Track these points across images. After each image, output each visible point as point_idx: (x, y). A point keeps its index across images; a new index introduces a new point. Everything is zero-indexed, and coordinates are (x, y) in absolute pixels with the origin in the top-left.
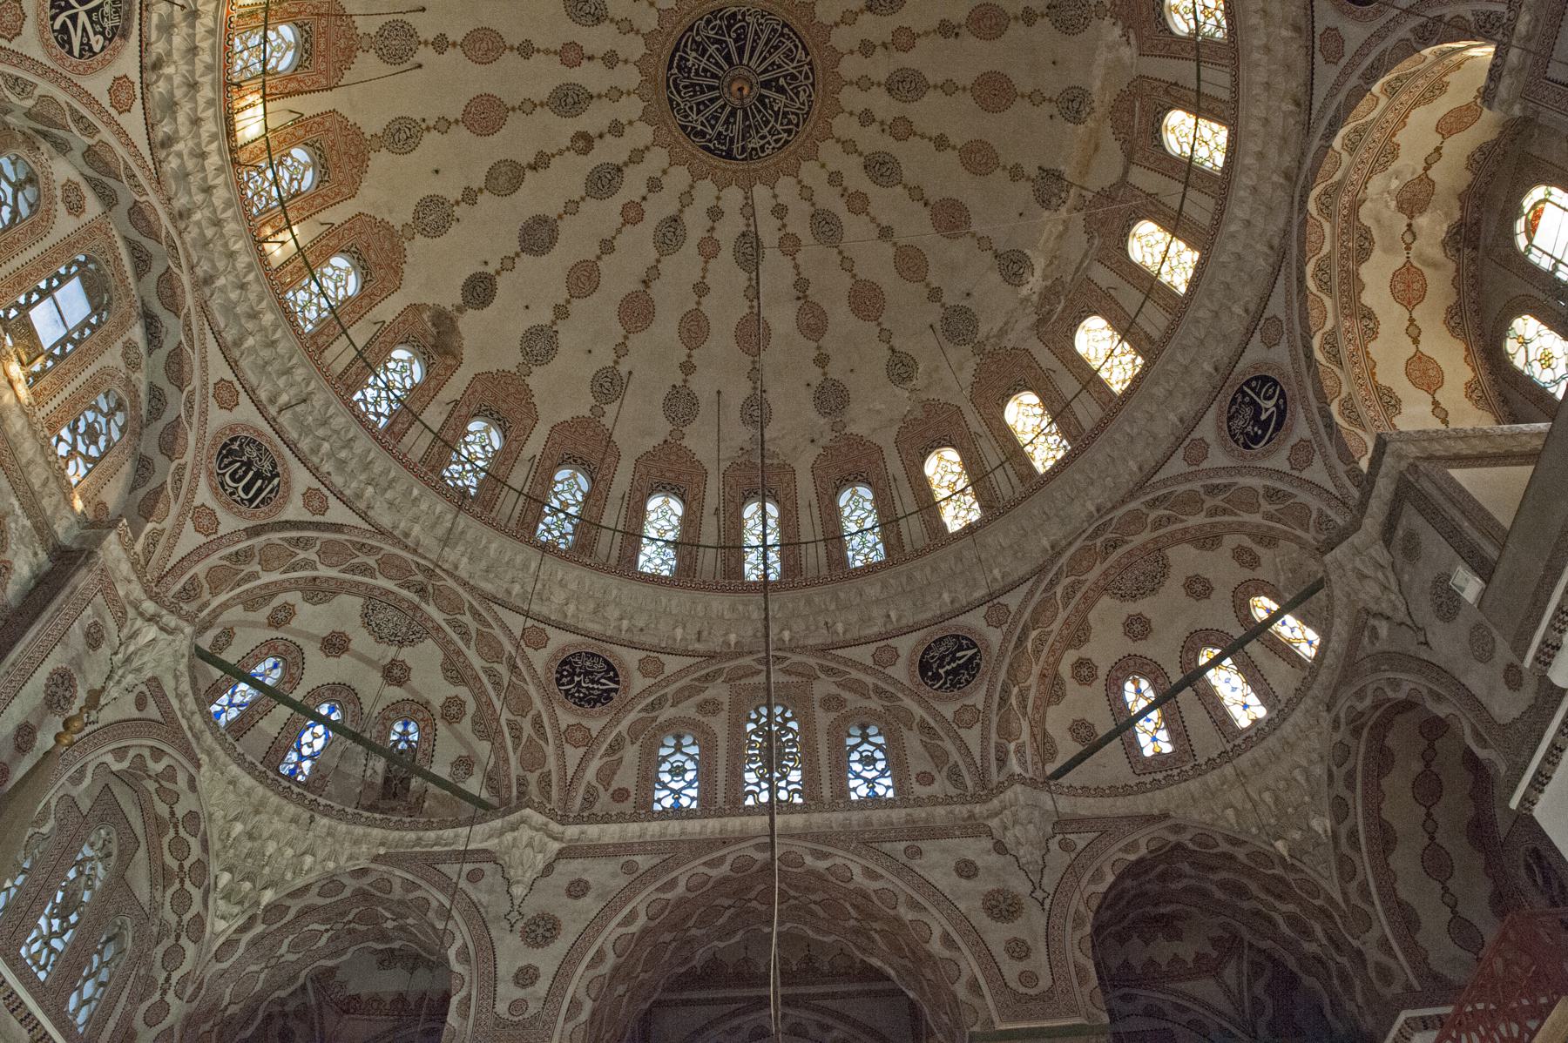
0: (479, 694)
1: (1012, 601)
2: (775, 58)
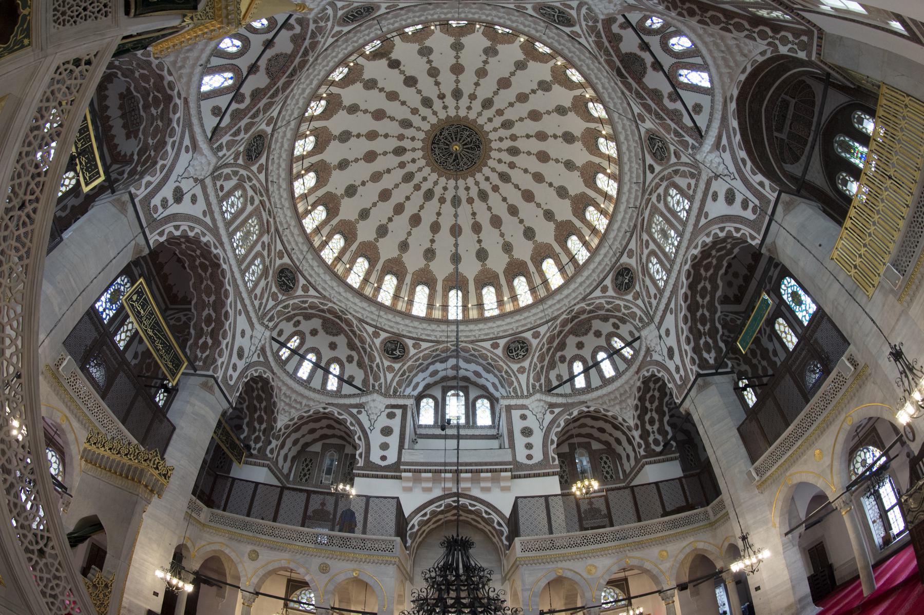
0: (248, 109)
1: (312, 292)
2: (465, 159)
